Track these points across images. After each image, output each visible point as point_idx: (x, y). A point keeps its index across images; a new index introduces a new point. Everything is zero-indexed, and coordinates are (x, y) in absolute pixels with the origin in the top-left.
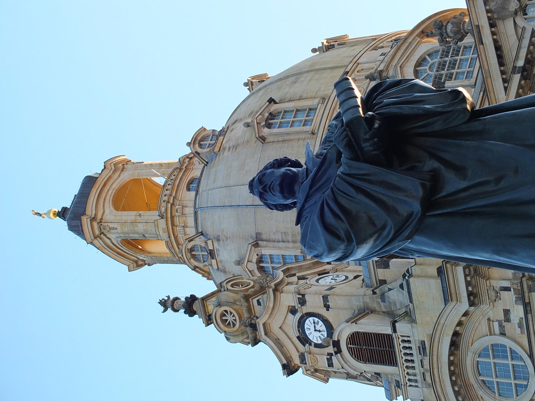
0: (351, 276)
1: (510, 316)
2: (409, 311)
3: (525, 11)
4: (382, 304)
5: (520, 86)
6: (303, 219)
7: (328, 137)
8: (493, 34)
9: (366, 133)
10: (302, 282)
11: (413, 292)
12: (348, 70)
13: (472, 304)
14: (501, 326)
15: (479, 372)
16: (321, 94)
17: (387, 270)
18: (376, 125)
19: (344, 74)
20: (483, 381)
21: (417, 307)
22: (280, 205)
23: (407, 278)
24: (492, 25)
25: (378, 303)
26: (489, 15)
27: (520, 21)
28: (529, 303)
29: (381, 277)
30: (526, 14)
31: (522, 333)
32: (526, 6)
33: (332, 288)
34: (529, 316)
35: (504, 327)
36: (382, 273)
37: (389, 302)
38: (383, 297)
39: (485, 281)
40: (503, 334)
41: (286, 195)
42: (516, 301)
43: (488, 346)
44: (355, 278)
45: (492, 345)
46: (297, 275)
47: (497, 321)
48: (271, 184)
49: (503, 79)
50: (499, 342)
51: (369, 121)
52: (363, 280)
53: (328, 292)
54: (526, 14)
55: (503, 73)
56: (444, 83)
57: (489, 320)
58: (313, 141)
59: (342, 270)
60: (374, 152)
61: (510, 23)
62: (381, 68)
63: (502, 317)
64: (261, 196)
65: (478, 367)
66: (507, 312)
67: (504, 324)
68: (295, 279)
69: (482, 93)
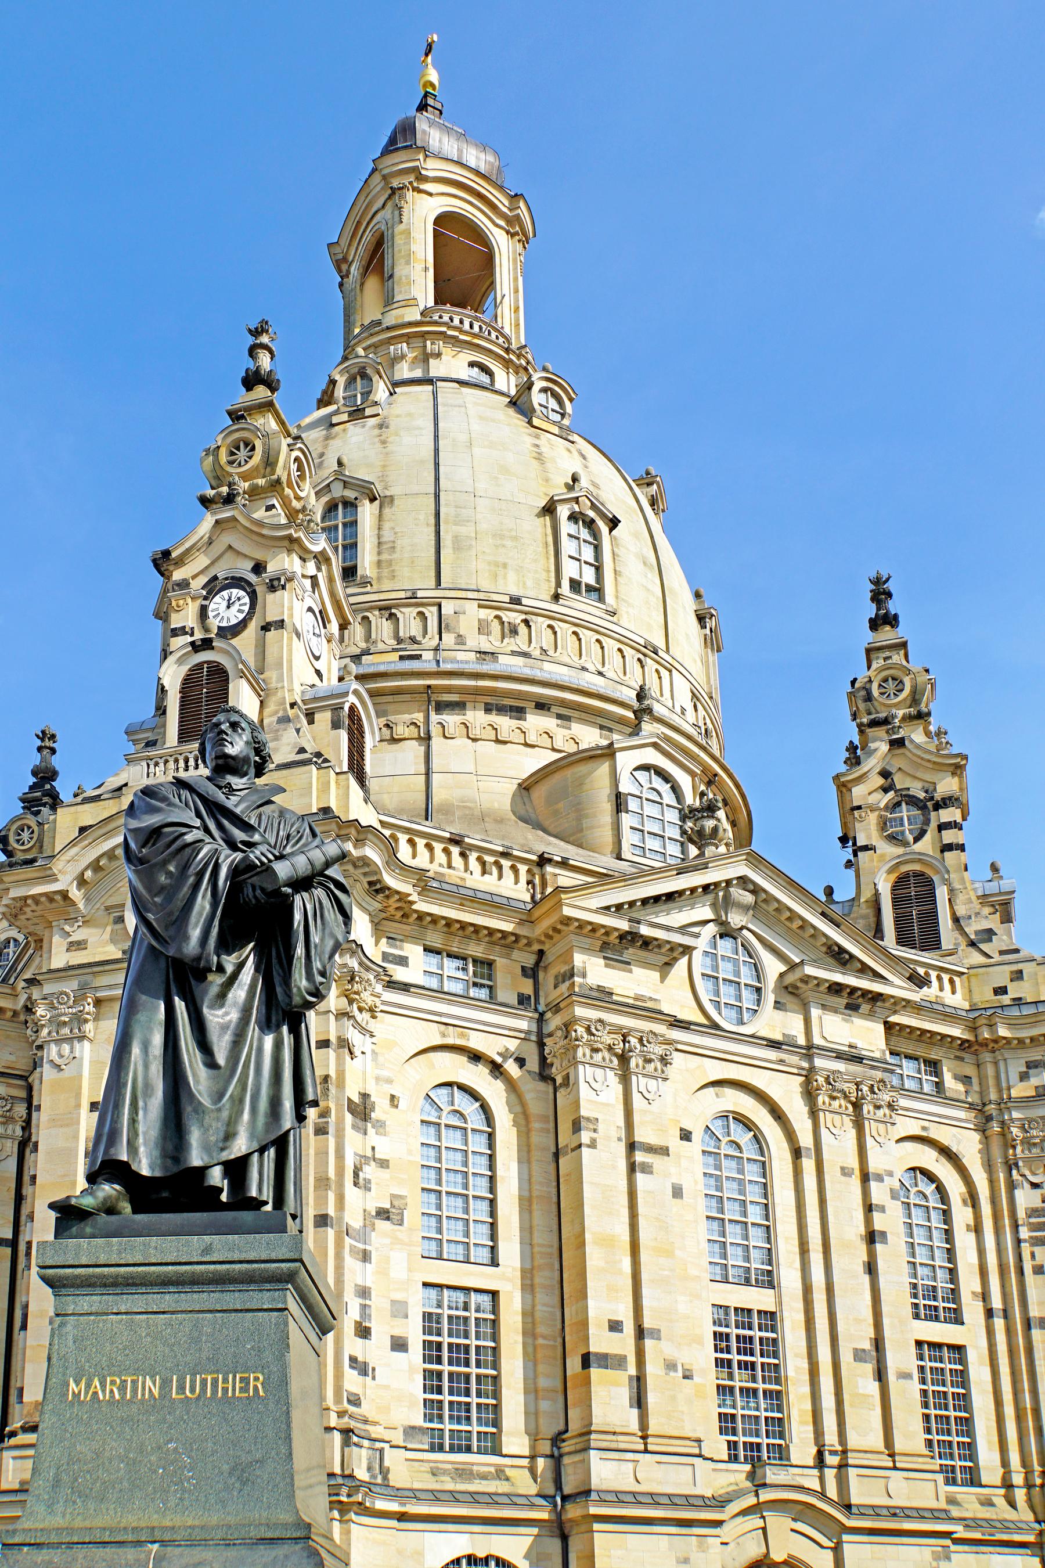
3: (727, 935)
5: (608, 931)
8: (693, 890)
12: (661, 653)
16: (623, 610)
24: (706, 888)
26: (723, 885)
27: (712, 929)
30: (721, 937)
32: (735, 938)
49: (622, 904)
54: (721, 937)
55: (632, 904)
56: (627, 812)
61: (707, 913)
62: (658, 709)
69: (605, 871)
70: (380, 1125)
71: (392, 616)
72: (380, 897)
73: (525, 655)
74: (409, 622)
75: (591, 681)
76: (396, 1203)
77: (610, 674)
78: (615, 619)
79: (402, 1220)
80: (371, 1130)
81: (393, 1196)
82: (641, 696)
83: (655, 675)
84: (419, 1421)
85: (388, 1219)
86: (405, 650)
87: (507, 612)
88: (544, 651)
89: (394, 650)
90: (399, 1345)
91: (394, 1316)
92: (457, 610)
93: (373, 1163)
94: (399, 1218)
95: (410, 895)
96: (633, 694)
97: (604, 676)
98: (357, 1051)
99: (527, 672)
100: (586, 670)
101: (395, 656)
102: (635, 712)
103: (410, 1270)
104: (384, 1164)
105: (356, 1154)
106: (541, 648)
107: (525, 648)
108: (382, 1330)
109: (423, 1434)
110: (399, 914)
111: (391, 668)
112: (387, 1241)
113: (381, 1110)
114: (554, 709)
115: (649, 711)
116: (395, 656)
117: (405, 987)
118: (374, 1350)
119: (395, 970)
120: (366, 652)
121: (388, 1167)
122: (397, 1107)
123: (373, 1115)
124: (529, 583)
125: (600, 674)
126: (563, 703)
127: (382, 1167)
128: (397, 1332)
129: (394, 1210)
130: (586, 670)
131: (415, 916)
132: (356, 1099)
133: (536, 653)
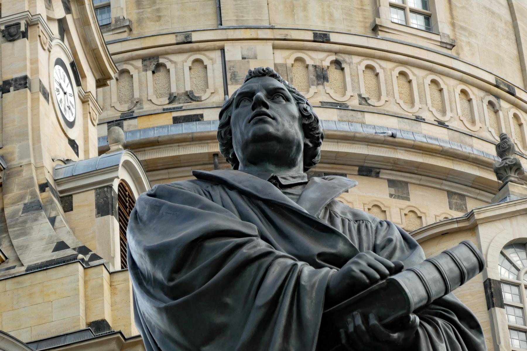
0: (75, 134)
2: (10, 265)
4: (20, 206)
6: (205, 185)
7: (366, 226)
9: (380, 319)
10: (54, 28)
11: (53, 273)
12: (518, 93)
16: (463, 40)
17: (94, 211)
18: (395, 335)
19: (508, 86)
21: (18, 283)
22: (230, 133)
23: (80, 256)
25: (22, 198)
29: (77, 199)
33: (46, 95)
36: (85, 202)
37: (25, 222)
38: (35, 207)
41: (251, 148)
44: (73, 144)
46: (69, 19)
48: (269, 116)
51: (403, 324)
52: (67, 161)
53: (35, 87)
56: (502, 305)
58: (359, 30)
59: (86, 113)
60: (343, 335)
64: (246, 96)
68: (59, 12)
71: (159, 66)
73: (341, 106)
74: (181, 73)
75: (429, 134)
77: (455, 124)
78: (453, 53)
82: (504, 148)
83: (512, 122)
86: (180, 109)
87: (311, 54)
88: (364, 100)
89: (165, 111)
92: (246, 53)
96: (492, 151)
97: (447, 127)
99: (345, 128)
100: (423, 120)
101: (168, 119)
102: (497, 172)
106: (360, 96)
107: (339, 98)
111: (163, 133)
114: (385, 175)
115: (517, 167)
116: (168, 119)
120: (128, 116)
124: (338, 14)
125: (441, 124)
126: (396, 166)
130: (423, 120)
133: (355, 103)
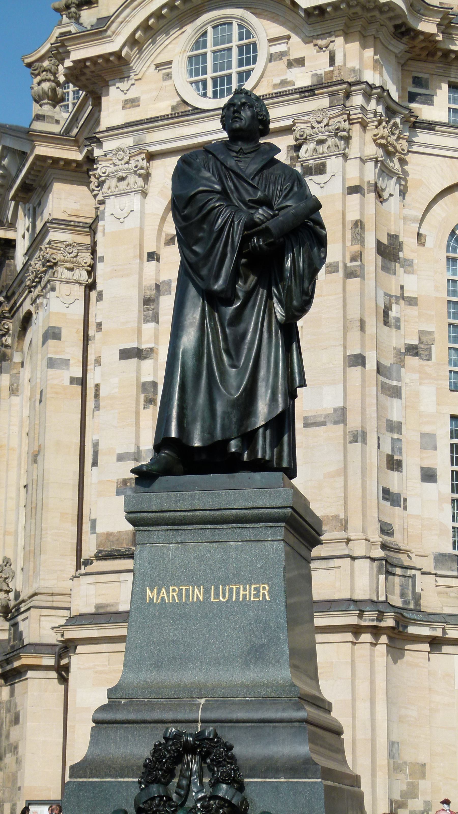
1: (295, 67)
13: (309, 12)
14: (282, 55)
15: (217, 26)
20: (206, 32)
28: (315, 95)
31: (275, 86)
34: (298, 96)
35: (281, 59)
39: (342, 28)
40: (271, 58)
42: (316, 75)
43: (253, 37)
45: (254, 44)
47: (289, 48)
50: (259, 54)
57: (288, 37)
60: (250, 247)
63: (294, 55)
65: (224, 24)
66: (300, 62)
67: (285, 59)
70: (408, 265)
72: (405, 39)
76: (424, 339)
79: (430, 355)
80: (400, 270)
81: (421, 333)
84: (448, 549)
85: (417, 354)
90: (429, 476)
91: (423, 447)
93: (402, 302)
94: (427, 353)
95: (432, 35)
98: (385, 195)
103: (438, 404)
104: (412, 301)
105: (386, 294)
108: (412, 463)
109: (452, 561)
110: (425, 53)
112: (416, 376)
113: (409, 249)
117: (430, 126)
118: (407, 482)
119: (420, 109)
121: (416, 304)
122: (424, 245)
123: (401, 255)
127: (411, 305)
128: (427, 464)
129: (422, 346)
131: (440, 54)
132: (385, 241)
